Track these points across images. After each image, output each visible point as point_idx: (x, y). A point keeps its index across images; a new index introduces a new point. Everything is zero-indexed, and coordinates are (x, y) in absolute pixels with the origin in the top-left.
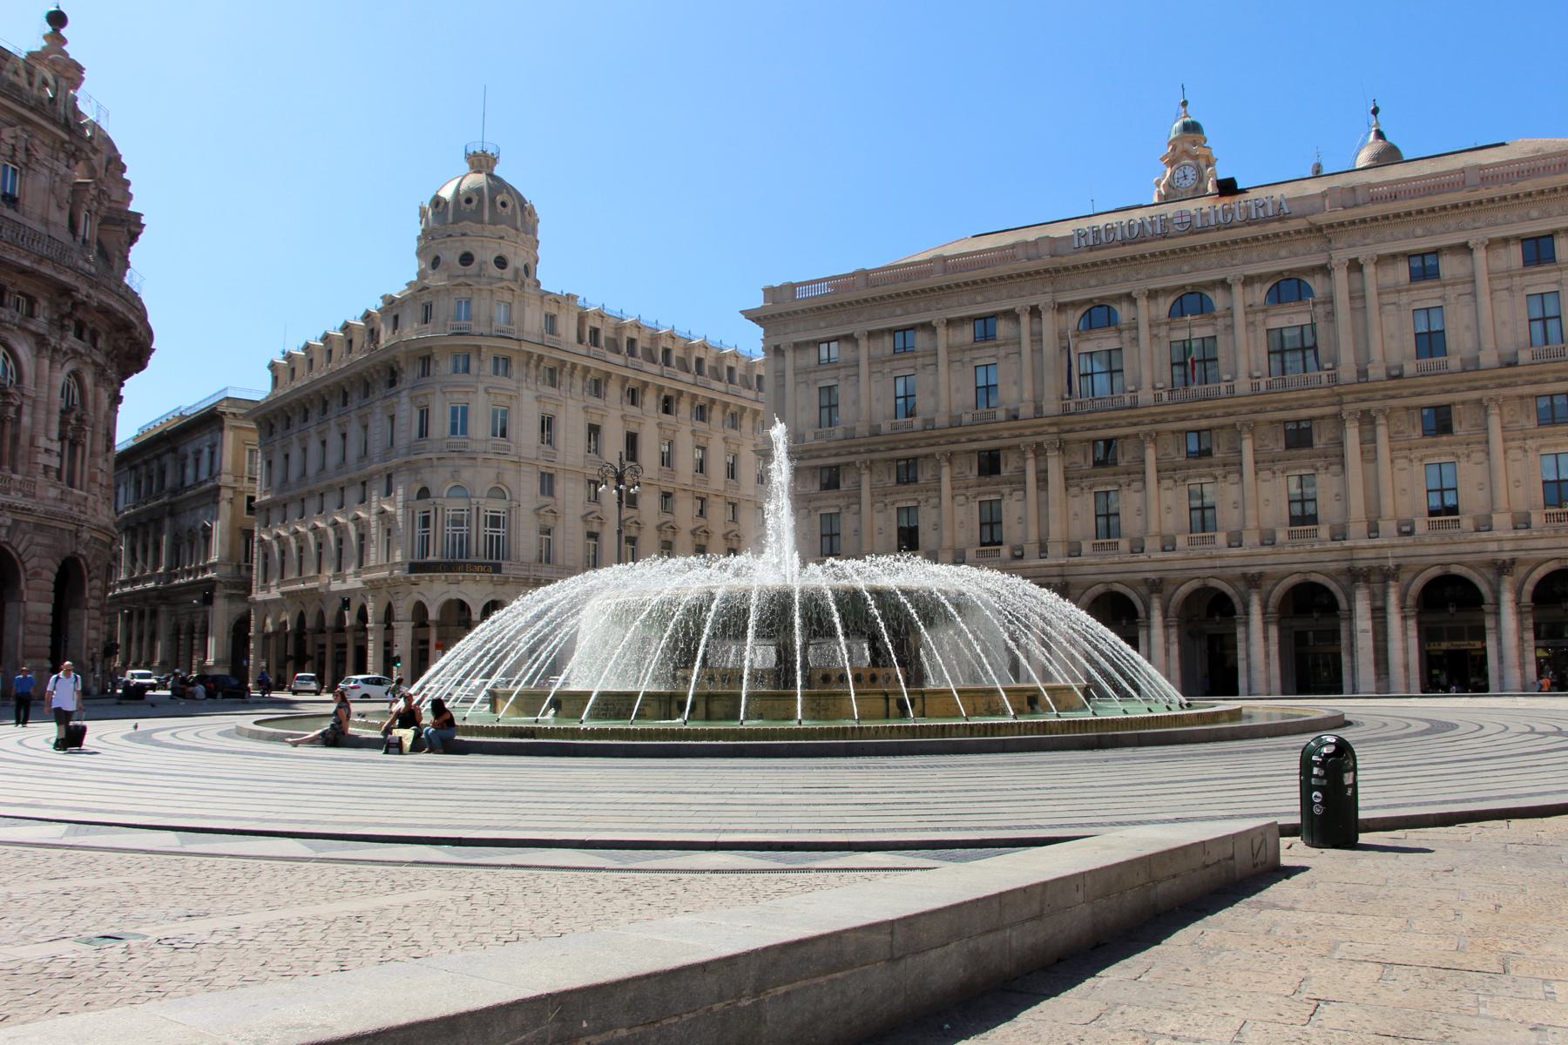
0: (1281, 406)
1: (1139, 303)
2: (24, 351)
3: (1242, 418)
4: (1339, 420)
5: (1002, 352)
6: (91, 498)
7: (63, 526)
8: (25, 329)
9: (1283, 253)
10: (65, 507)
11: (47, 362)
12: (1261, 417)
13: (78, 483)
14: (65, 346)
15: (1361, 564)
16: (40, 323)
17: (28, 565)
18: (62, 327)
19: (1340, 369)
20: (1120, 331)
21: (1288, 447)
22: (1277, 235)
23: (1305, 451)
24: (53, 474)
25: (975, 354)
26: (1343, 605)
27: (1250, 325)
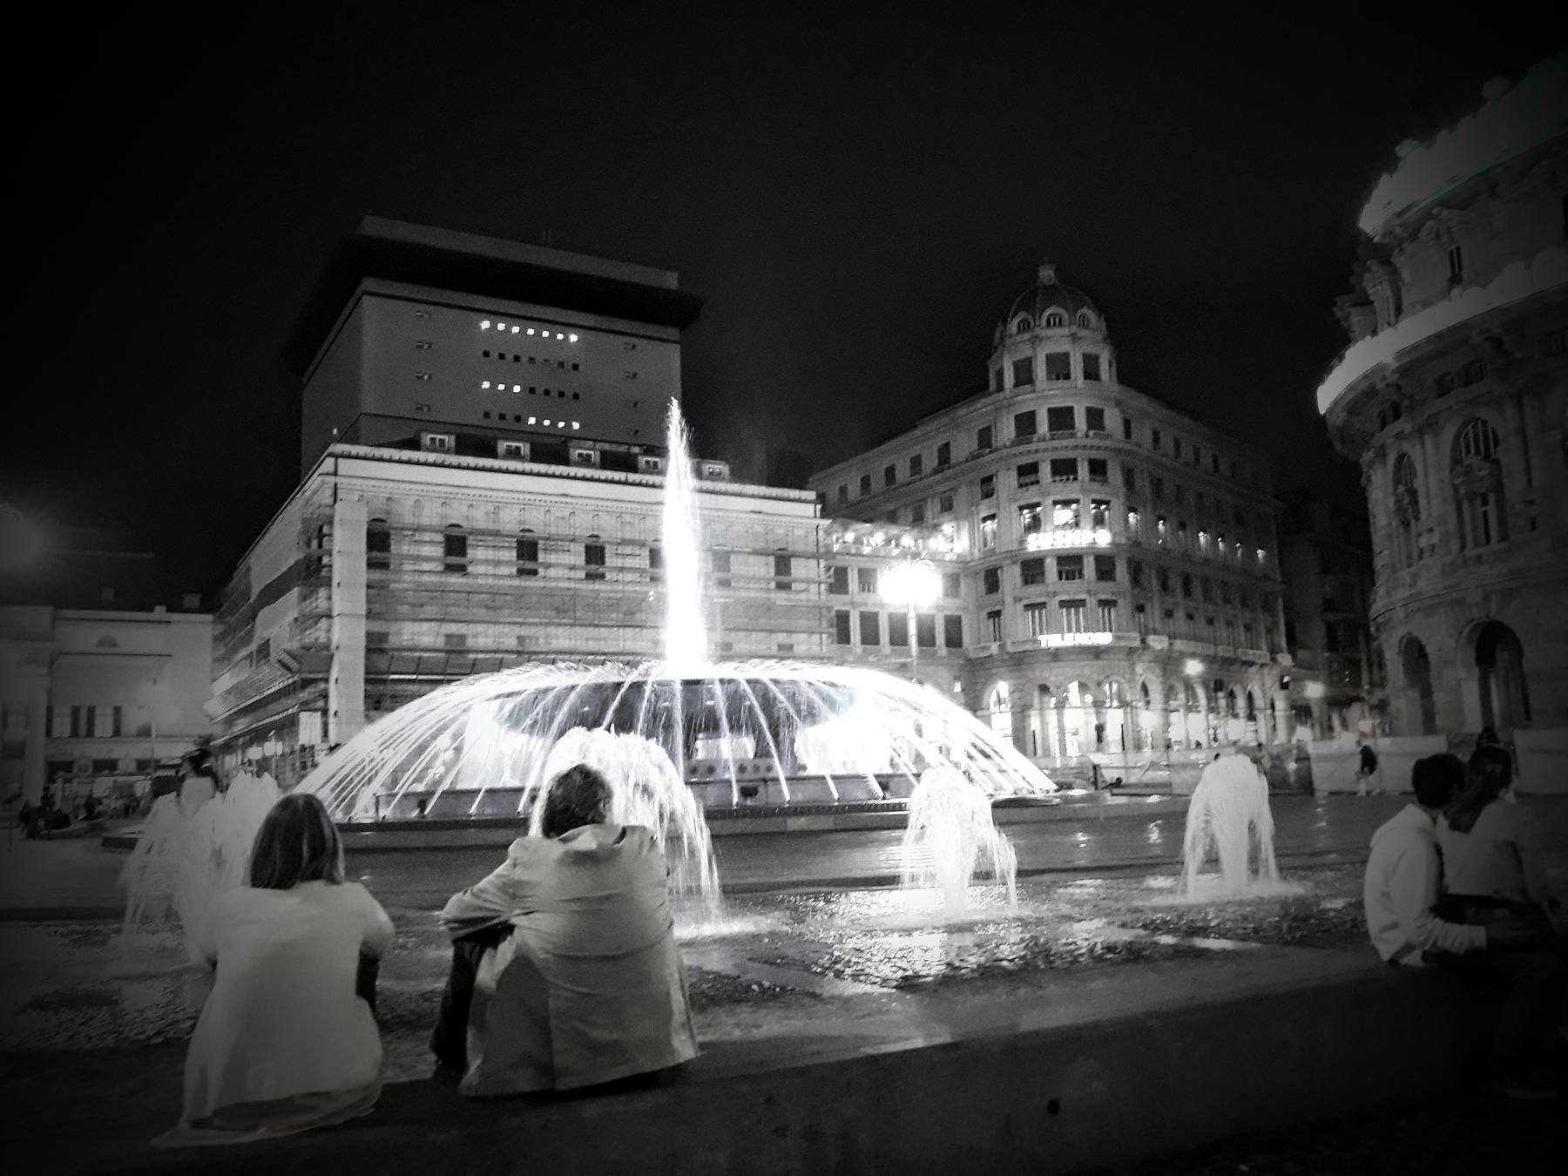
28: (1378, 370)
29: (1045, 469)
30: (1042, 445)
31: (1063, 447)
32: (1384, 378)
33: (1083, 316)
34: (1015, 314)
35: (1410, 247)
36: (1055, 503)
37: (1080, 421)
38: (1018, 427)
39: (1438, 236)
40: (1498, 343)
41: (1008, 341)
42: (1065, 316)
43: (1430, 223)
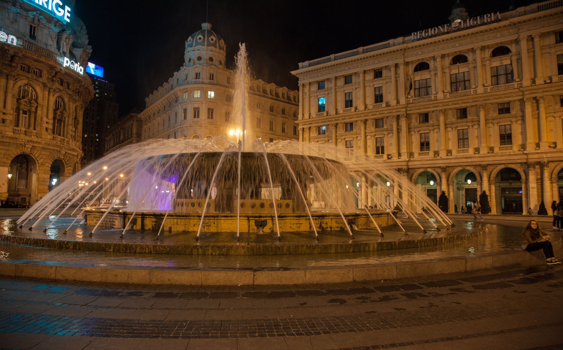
0: (497, 97)
1: (438, 60)
2: (38, 89)
3: (480, 103)
4: (522, 102)
5: (384, 82)
6: (66, 139)
7: (54, 148)
8: (38, 81)
9: (499, 35)
10: (55, 142)
11: (47, 93)
12: (488, 102)
13: (62, 134)
14: (54, 87)
15: (530, 161)
16: (44, 79)
17: (39, 162)
18: (53, 80)
19: (523, 81)
20: (430, 71)
21: (499, 114)
22: (495, 29)
23: (507, 115)
24: (50, 131)
25: (374, 83)
26: (523, 177)
27: (484, 66)
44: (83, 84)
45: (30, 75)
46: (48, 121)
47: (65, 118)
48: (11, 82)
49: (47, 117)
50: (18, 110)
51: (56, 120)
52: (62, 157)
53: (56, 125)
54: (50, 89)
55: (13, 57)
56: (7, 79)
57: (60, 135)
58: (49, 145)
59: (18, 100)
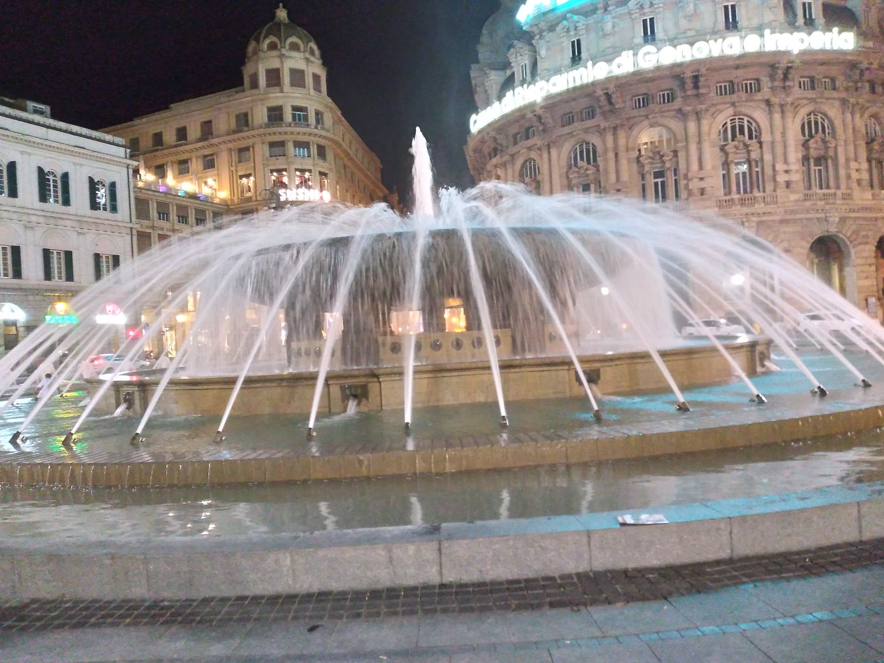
8: (754, 100)
11: (777, 116)
13: (832, 183)
16: (766, 92)
24: (801, 186)
28: (531, 106)
29: (290, 147)
30: (289, 129)
31: (301, 132)
32: (534, 111)
33: (311, 48)
34: (265, 38)
35: (548, 36)
36: (296, 170)
37: (312, 119)
38: (269, 117)
39: (568, 31)
40: (608, 96)
41: (261, 54)
42: (302, 46)
43: (565, 23)
44: (865, 65)
45: (734, 97)
46: (785, 167)
47: (836, 148)
48: (705, 123)
49: (786, 161)
50: (726, 164)
51: (812, 162)
52: (833, 230)
53: (813, 167)
54: (782, 106)
55: (696, 78)
56: (699, 120)
57: (828, 187)
58: (792, 212)
59: (723, 149)
